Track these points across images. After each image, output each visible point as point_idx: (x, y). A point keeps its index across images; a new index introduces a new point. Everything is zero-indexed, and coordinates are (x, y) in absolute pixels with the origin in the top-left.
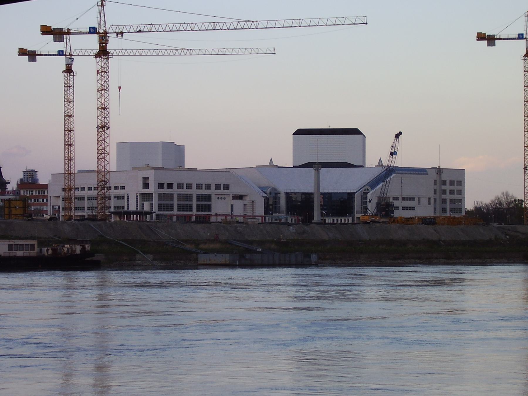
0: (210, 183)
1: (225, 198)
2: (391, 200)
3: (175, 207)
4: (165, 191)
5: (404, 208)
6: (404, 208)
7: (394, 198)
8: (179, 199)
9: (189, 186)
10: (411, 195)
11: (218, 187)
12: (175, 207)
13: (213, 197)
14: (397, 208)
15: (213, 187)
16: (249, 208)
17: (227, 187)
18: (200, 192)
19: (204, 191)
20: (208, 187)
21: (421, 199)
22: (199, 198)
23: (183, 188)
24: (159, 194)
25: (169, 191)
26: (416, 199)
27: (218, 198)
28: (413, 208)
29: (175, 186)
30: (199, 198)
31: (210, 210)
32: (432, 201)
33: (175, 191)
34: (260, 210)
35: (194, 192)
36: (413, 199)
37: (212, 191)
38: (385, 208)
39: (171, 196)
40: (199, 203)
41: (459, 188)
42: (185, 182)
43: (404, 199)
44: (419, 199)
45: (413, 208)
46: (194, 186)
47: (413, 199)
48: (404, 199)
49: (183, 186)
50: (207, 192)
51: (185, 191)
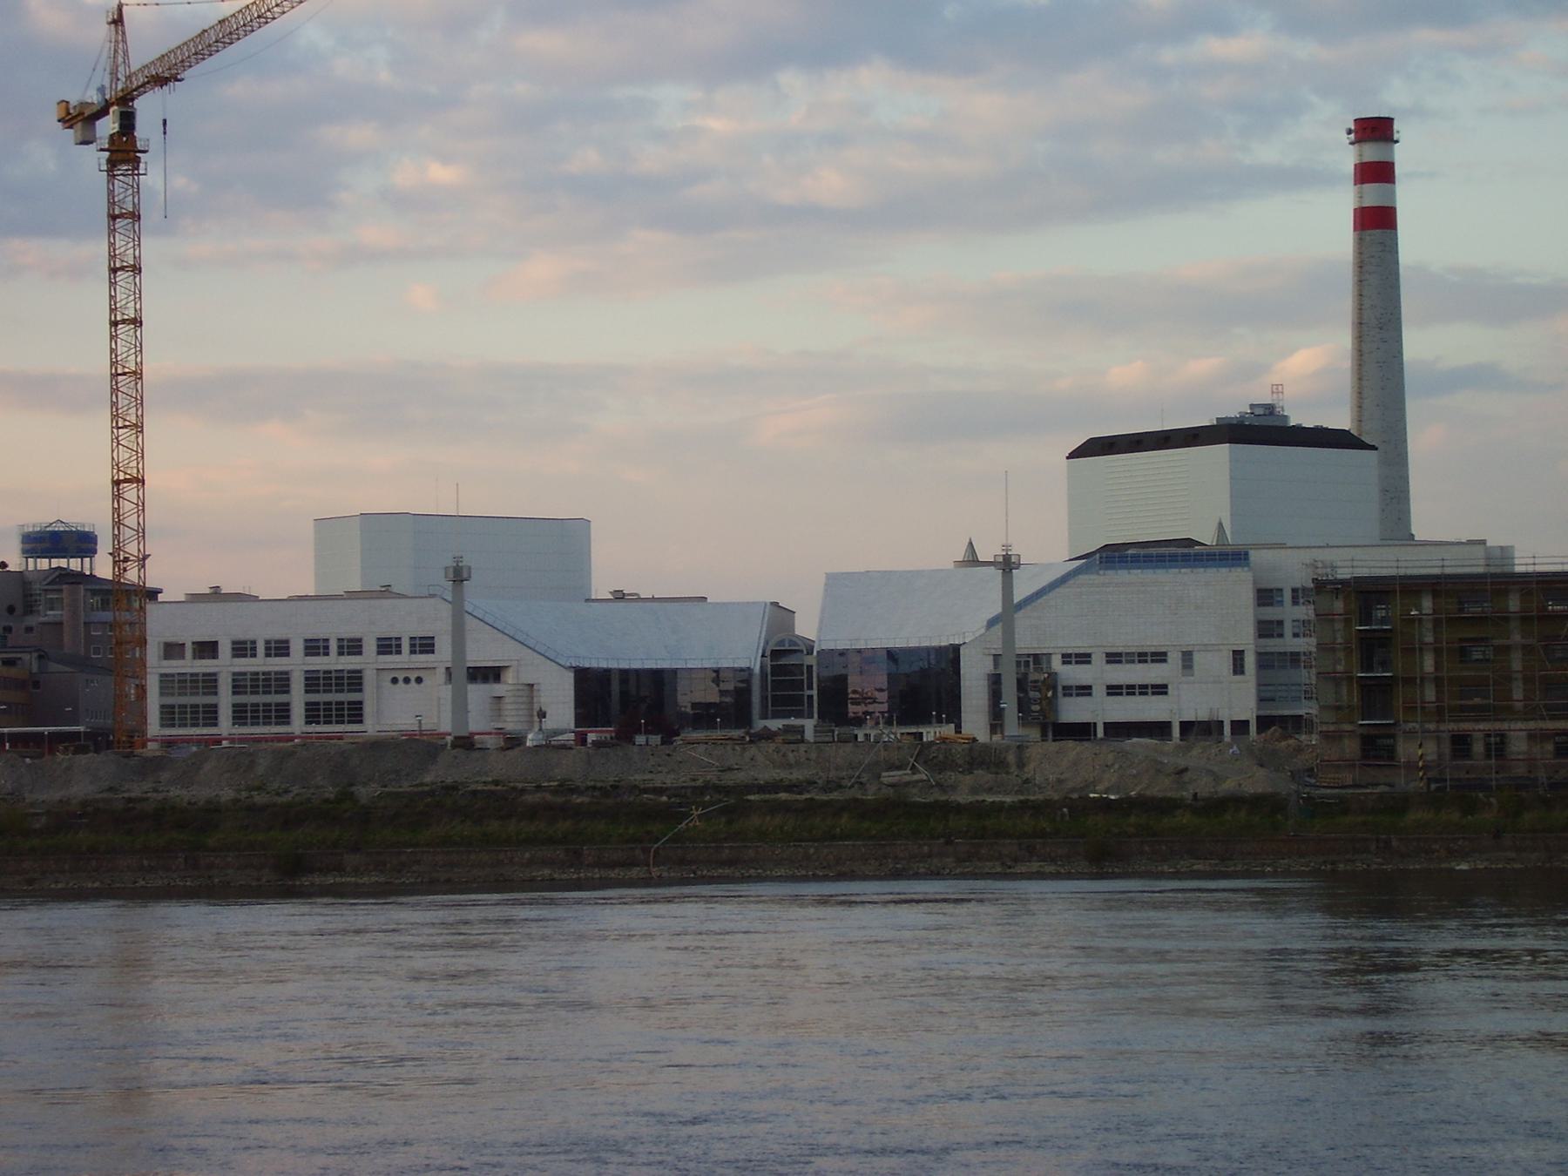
0: (358, 635)
1: (419, 680)
2: (1056, 664)
3: (225, 714)
5: (1114, 690)
6: (1114, 690)
7: (1067, 659)
8: (237, 688)
9: (280, 648)
10: (1152, 644)
11: (387, 646)
12: (225, 714)
13: (369, 679)
14: (1085, 690)
15: (370, 647)
17: (425, 645)
18: (319, 663)
20: (352, 647)
21: (1197, 657)
22: (313, 681)
23: (254, 655)
24: (162, 675)
25: (204, 666)
26: (1174, 658)
27: (395, 681)
28: (1161, 690)
29: (225, 649)
32: (1250, 661)
34: (561, 711)
35: (297, 664)
36: (1160, 657)
37: (369, 662)
40: (170, 701)
42: (262, 633)
43: (1113, 658)
44: (1187, 658)
45: (1161, 690)
46: (297, 647)
47: (1160, 657)
48: (1113, 658)
49: (254, 649)
50: (348, 663)
51: (259, 664)
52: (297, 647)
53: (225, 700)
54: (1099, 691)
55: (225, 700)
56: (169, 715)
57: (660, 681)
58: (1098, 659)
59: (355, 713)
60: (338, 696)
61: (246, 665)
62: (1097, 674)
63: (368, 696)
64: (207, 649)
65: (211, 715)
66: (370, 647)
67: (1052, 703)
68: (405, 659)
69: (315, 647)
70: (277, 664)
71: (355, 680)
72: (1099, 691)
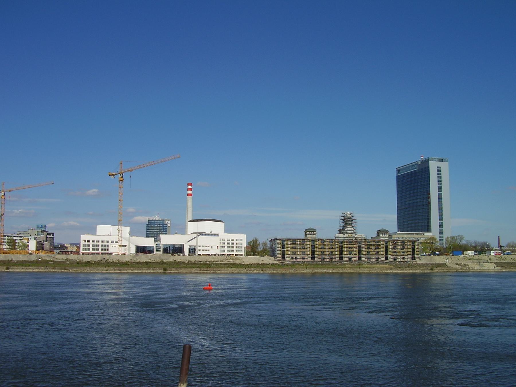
4: (87, 243)
5: (203, 250)
6: (203, 250)
8: (93, 246)
9: (98, 242)
14: (200, 250)
15: (110, 242)
16: (127, 250)
18: (103, 244)
19: (105, 244)
20: (108, 242)
25: (88, 243)
26: (210, 247)
28: (209, 250)
29: (91, 241)
30: (102, 246)
31: (108, 251)
33: (91, 243)
34: (133, 250)
35: (100, 244)
36: (209, 246)
37: (109, 243)
38: (193, 251)
39: (89, 246)
41: (241, 242)
43: (203, 246)
45: (209, 250)
46: (100, 242)
47: (209, 246)
48: (203, 246)
50: (107, 244)
51: (96, 243)
52: (100, 242)
53: (91, 248)
54: (201, 250)
55: (91, 248)
56: (83, 250)
57: (144, 247)
58: (201, 246)
59: (108, 250)
60: (106, 248)
61: (94, 243)
62: (201, 248)
63: (109, 248)
64: (89, 241)
65: (89, 250)
66: (110, 242)
67: (196, 252)
68: (114, 243)
69: (102, 242)
70: (98, 244)
71: (108, 246)
72: (201, 250)
